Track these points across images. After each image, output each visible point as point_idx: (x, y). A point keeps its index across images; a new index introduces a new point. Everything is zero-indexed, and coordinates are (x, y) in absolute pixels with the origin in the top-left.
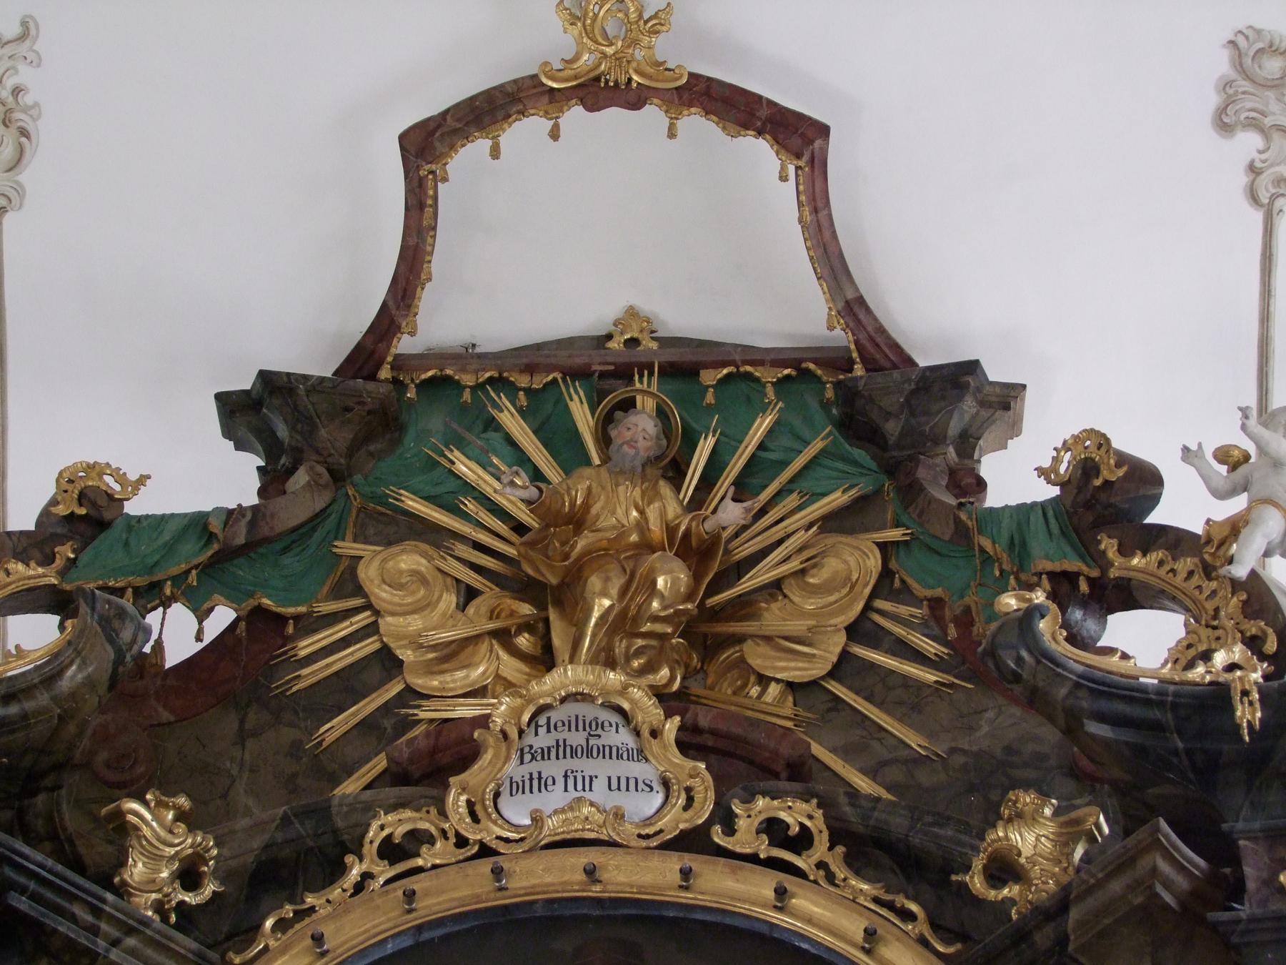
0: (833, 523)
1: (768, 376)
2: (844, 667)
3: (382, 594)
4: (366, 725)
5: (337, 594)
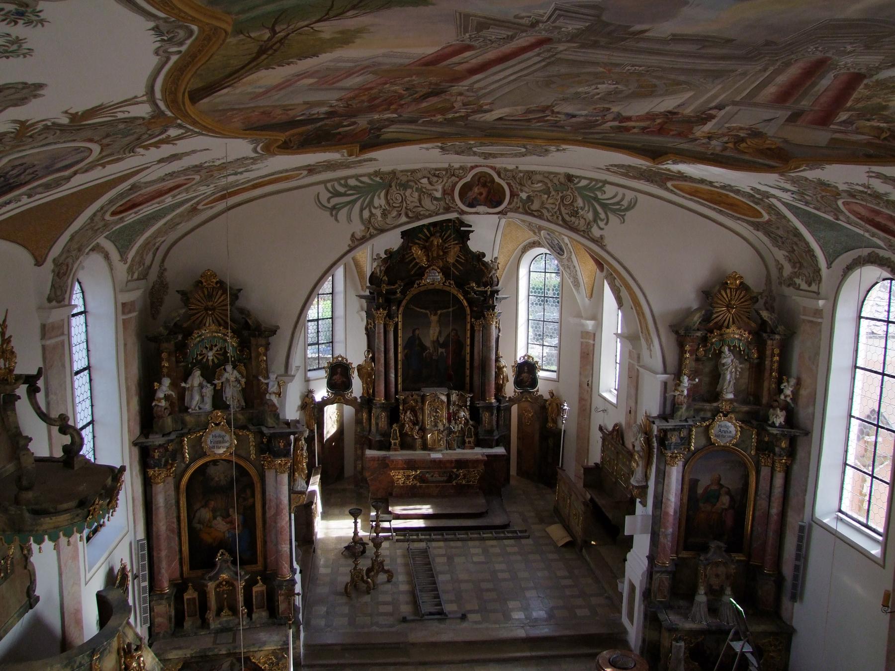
0: (457, 244)
2: (457, 261)
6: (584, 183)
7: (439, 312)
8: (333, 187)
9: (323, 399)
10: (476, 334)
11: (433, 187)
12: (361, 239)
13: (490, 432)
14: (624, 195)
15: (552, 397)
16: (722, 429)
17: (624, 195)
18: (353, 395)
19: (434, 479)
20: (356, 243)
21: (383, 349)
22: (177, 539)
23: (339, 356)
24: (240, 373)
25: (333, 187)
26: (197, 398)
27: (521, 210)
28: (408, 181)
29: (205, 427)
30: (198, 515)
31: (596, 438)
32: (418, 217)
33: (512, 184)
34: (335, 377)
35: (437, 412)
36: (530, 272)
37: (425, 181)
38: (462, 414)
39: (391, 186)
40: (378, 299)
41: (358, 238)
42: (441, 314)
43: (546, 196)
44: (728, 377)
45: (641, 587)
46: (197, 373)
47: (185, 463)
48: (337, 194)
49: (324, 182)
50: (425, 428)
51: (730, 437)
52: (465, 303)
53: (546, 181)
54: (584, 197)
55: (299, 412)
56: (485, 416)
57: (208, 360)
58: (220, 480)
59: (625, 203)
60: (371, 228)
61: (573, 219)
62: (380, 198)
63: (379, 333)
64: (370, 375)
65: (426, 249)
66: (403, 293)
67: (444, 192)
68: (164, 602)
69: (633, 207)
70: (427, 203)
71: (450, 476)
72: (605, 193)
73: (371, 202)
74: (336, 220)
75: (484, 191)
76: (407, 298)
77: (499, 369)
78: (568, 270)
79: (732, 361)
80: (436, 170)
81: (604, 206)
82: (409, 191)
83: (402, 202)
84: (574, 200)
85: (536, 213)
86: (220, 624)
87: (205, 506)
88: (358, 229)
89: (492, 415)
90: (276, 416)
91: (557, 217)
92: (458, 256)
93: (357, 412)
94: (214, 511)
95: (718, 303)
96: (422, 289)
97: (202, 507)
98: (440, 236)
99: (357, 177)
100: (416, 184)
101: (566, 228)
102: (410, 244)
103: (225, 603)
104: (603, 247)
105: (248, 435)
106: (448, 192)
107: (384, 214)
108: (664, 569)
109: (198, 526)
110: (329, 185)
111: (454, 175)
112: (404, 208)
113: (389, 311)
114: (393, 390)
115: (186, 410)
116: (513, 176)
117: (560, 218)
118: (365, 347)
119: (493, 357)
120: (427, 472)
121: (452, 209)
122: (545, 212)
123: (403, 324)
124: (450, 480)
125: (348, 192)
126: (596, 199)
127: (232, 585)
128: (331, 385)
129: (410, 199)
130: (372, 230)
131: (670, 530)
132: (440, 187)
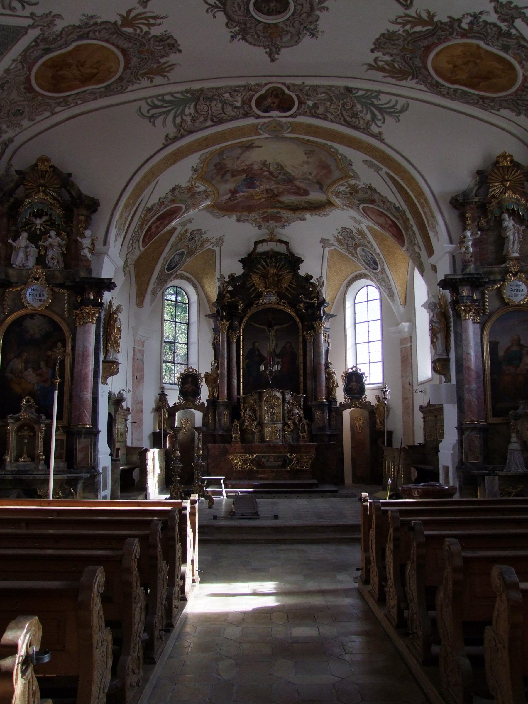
0: (288, 272)
1: (283, 257)
2: (289, 286)
4: (253, 290)
6: (360, 93)
7: (275, 328)
8: (152, 102)
9: (175, 404)
10: (308, 345)
11: (234, 99)
12: (173, 139)
13: (322, 428)
14: (397, 101)
15: (378, 401)
16: (513, 288)
17: (397, 101)
18: (201, 401)
19: (269, 464)
20: (169, 141)
24: (62, 239)
25: (152, 102)
26: (21, 255)
27: (308, 114)
28: (213, 96)
29: (26, 283)
31: (419, 416)
32: (221, 122)
33: (300, 95)
34: (186, 386)
35: (273, 409)
36: (355, 304)
37: (227, 95)
38: (297, 411)
39: (199, 100)
40: (222, 312)
41: (171, 137)
42: (277, 330)
43: (329, 103)
44: (511, 238)
45: (453, 464)
46: (25, 235)
47: (4, 313)
48: (156, 107)
49: (146, 99)
50: (263, 423)
51: (522, 295)
52: (298, 320)
53: (328, 92)
54: (362, 104)
55: (153, 414)
56: (318, 414)
57: (36, 228)
59: (399, 107)
60: (182, 130)
61: (354, 120)
62: (190, 108)
63: (223, 341)
64: (215, 380)
65: (264, 277)
66: (245, 310)
67: (243, 103)
69: (406, 110)
70: (229, 111)
71: (285, 461)
72: (380, 100)
73: (182, 113)
74: (154, 125)
75: (277, 101)
77: (329, 376)
78: (383, 284)
79: (513, 225)
80: (236, 87)
81: (381, 110)
82: (214, 103)
83: (208, 110)
84: (354, 106)
85: (321, 116)
86: (16, 467)
88: (172, 131)
89: (323, 413)
90: (89, 271)
91: (340, 119)
92: (290, 283)
95: (491, 179)
96: (261, 308)
98: (275, 266)
99: (172, 94)
100: (220, 97)
101: (348, 127)
102: (250, 274)
103: (25, 448)
104: (382, 141)
105: (64, 293)
106: (246, 103)
107: (193, 120)
108: (472, 426)
109: (9, 375)
110: (149, 101)
111: (251, 90)
112: (210, 114)
114: (236, 393)
115: (11, 266)
116: (301, 90)
117: (342, 119)
118: (212, 358)
119: (323, 362)
120: (263, 456)
121: (249, 115)
122: (329, 115)
123: (244, 338)
124: (284, 465)
125: (165, 105)
126: (373, 104)
127: (32, 429)
128: (182, 393)
129: (214, 108)
130: (182, 131)
131: (474, 386)
132: (240, 99)
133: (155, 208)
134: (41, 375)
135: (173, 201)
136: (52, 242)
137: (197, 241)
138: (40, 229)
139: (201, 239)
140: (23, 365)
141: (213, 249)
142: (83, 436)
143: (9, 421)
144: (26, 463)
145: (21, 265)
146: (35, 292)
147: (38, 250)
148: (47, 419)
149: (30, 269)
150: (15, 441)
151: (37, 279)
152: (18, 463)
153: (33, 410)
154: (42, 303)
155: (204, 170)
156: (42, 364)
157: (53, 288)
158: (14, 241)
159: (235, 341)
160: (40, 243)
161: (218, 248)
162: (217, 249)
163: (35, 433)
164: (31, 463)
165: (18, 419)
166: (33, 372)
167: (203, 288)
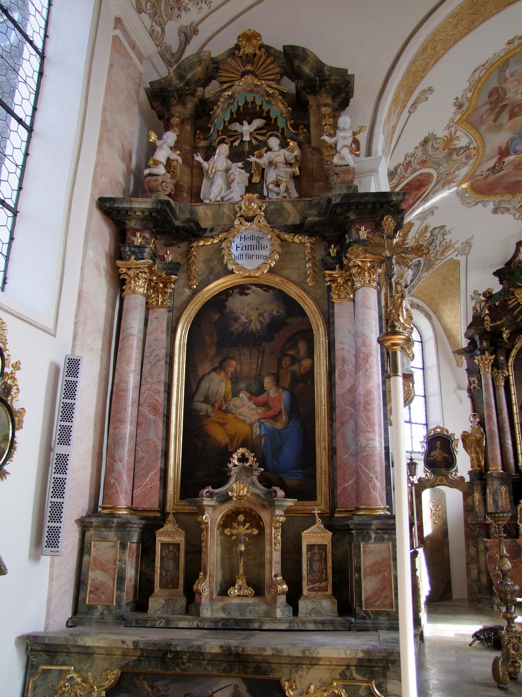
3: (518, 296)
5: (512, 296)
18: (459, 474)
21: (493, 404)
22: (161, 426)
23: (437, 428)
26: (219, 182)
29: (229, 229)
30: (205, 385)
34: (433, 453)
46: (223, 150)
58: (250, 322)
68: (112, 535)
76: (517, 346)
86: (224, 609)
87: (220, 368)
93: (467, 495)
94: (235, 379)
97: (214, 370)
102: (511, 289)
103: (241, 564)
109: (204, 407)
113: (496, 360)
128: (430, 463)
133: (399, 172)
134: (265, 405)
135: (423, 163)
136: (273, 157)
137: (438, 245)
138: (250, 142)
139: (444, 243)
140: (229, 386)
141: (456, 259)
142: (373, 536)
143: (207, 502)
144: (245, 601)
145: (219, 199)
146: (249, 242)
147: (248, 175)
148: (286, 497)
149: (237, 203)
150: (219, 548)
151: (250, 220)
152: (228, 601)
153: (255, 478)
154: (261, 261)
155: (473, 103)
156: (268, 382)
157: (282, 234)
158: (207, 159)
159: (503, 384)
160: (252, 159)
161: (464, 257)
162: (462, 259)
163: (262, 529)
164: (256, 599)
165: (226, 499)
166: (250, 399)
167: (440, 319)
